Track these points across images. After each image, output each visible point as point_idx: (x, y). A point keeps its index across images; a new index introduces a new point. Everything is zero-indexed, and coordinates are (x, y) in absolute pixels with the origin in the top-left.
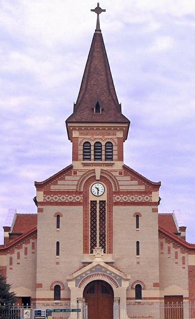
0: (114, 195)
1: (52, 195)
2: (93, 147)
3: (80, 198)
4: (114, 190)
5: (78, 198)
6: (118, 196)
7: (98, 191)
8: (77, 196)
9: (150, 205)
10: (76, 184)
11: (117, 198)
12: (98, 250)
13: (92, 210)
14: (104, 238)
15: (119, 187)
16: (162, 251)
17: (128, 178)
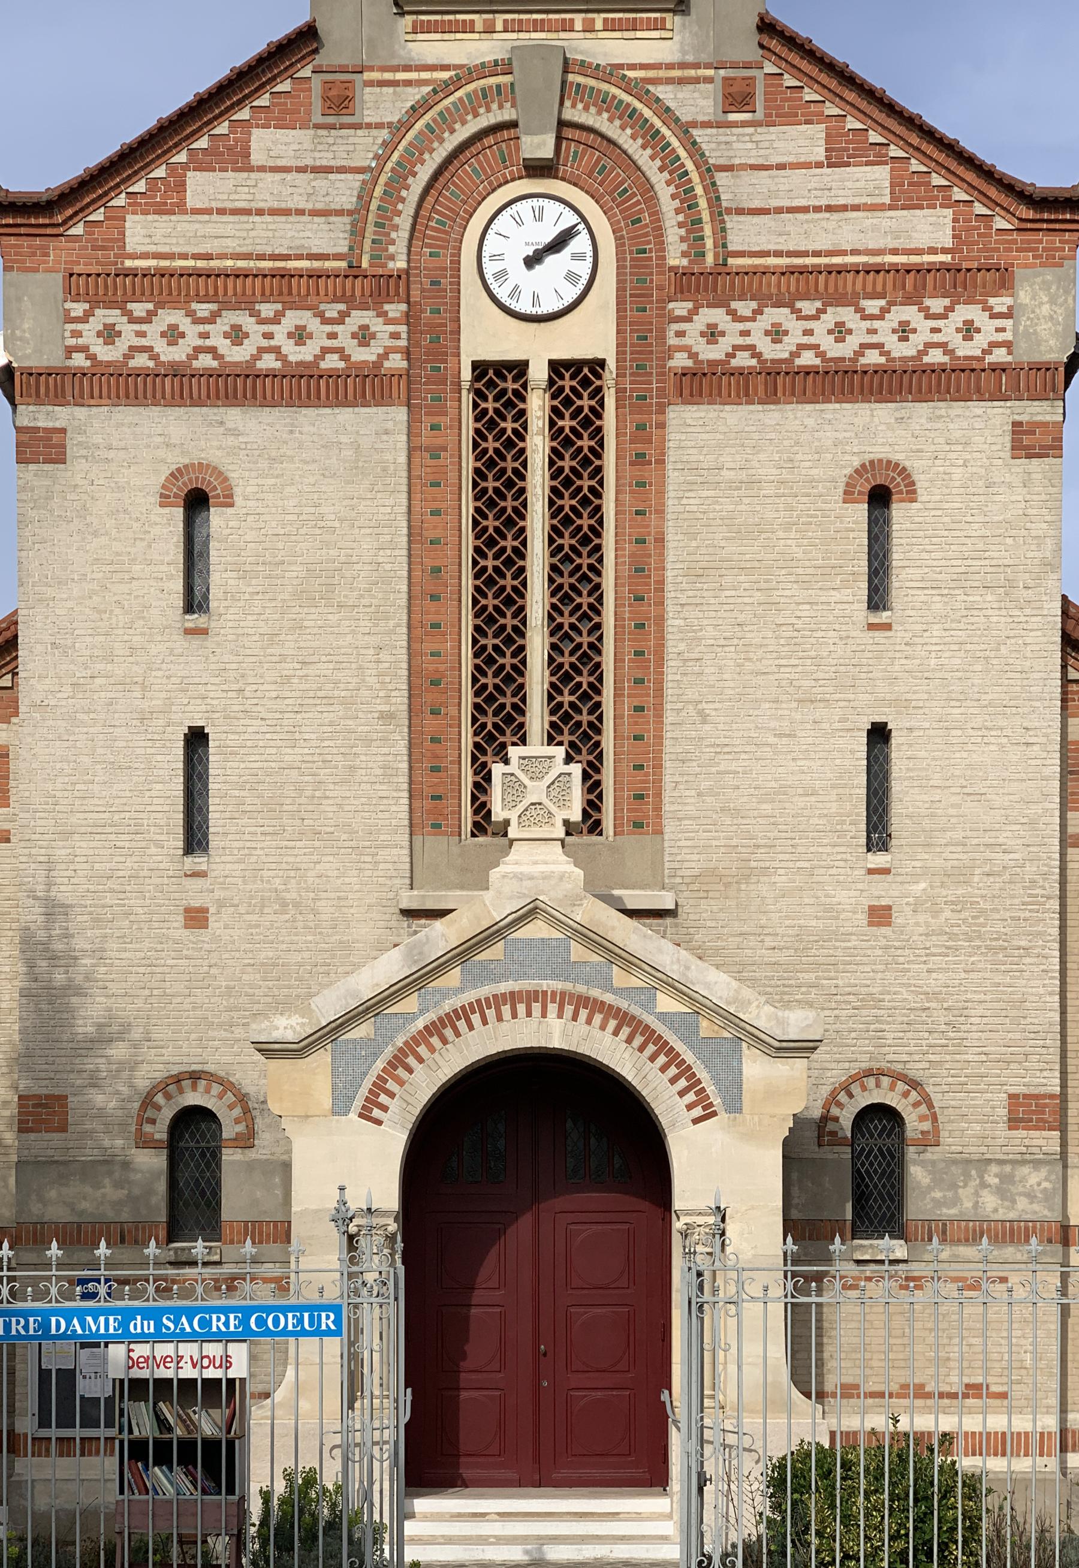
0: (680, 308)
1: (139, 309)
3: (378, 337)
4: (675, 258)
5: (364, 337)
6: (716, 315)
8: (359, 318)
9: (998, 396)
11: (700, 334)
13: (491, 445)
15: (721, 231)
17: (807, 140)
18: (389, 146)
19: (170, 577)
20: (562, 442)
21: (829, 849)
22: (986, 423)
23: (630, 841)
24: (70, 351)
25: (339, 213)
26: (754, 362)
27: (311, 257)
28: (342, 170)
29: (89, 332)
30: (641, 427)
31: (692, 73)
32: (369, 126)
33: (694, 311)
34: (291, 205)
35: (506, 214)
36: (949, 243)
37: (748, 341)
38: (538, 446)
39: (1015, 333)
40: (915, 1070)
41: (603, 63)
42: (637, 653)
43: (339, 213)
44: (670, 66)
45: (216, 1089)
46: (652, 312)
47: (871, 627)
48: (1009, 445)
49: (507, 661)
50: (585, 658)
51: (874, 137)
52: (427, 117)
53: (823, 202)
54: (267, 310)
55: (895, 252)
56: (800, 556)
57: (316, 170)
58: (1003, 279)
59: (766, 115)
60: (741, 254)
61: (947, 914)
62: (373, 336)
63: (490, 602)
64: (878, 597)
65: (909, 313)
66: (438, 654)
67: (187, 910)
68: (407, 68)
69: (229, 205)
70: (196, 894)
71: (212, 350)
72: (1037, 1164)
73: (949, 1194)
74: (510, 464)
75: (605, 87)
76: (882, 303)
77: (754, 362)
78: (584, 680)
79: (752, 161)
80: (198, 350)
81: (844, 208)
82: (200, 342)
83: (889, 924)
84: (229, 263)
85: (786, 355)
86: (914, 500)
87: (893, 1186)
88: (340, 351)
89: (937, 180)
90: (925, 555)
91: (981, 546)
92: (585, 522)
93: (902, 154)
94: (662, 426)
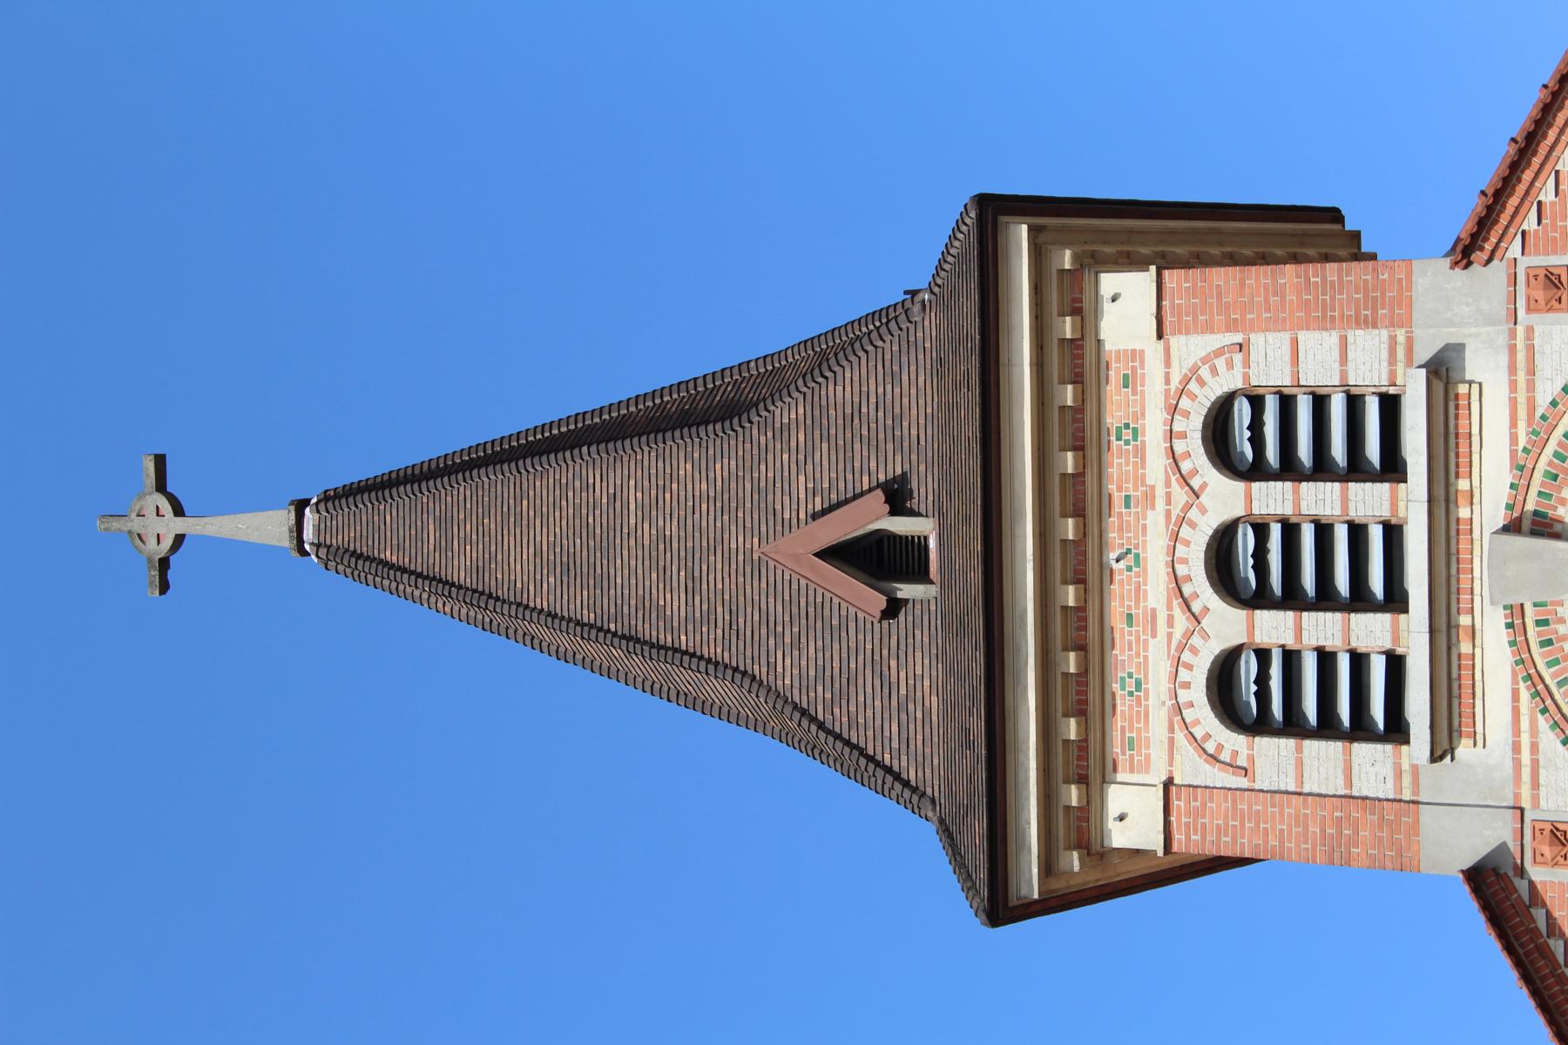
2: (1264, 617)
31: (1521, 356)
41: (1509, 480)
44: (1513, 386)
68: (1516, 748)
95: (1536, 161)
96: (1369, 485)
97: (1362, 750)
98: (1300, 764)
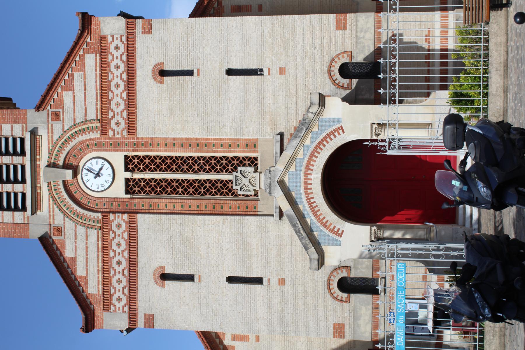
0: (111, 133)
1: (112, 291)
3: (118, 222)
5: (119, 226)
6: (113, 122)
7: (104, 177)
8: (114, 228)
10: (84, 229)
12: (246, 180)
14: (218, 160)
16: (255, 7)
17: (67, 96)
18: (69, 217)
19: (185, 285)
20: (147, 168)
21: (263, 87)
22: (143, 42)
23: (260, 148)
24: (124, 311)
25: (87, 232)
26: (125, 111)
27: (98, 241)
28: (76, 231)
29: (119, 305)
30: (143, 144)
31: (50, 130)
32: (64, 223)
33: (112, 129)
34: (85, 246)
35: (87, 184)
36: (94, 55)
37: (120, 113)
38: (148, 176)
39: (117, 34)
40: (329, 60)
41: (48, 156)
42: (206, 146)
43: (87, 232)
44: (49, 136)
45: (332, 278)
46: (112, 141)
47: (198, 75)
48: (148, 35)
49: (208, 185)
50: (207, 162)
51: (66, 77)
52: (62, 206)
53: (83, 92)
54: (112, 254)
55: (96, 70)
56: (178, 97)
57: (76, 239)
58: (103, 39)
59: (61, 108)
60: (97, 115)
61: (282, 50)
62: (119, 223)
63: (191, 190)
64: (190, 73)
65: (112, 65)
66: (206, 206)
67: (279, 284)
68: (50, 212)
69: (85, 264)
70: (274, 282)
71: (123, 270)
72: (357, 21)
73: (366, 48)
74: (153, 184)
75: (54, 155)
76: (110, 74)
77: (125, 111)
78: (213, 162)
79: (73, 112)
80: (123, 274)
81: (85, 85)
82: (121, 274)
83: (285, 68)
84: (100, 264)
85: (123, 102)
86: (163, 63)
87: (364, 65)
88: (123, 233)
89: (77, 59)
90: (178, 59)
91: (176, 42)
92: (169, 161)
93: (71, 69)
94: (142, 138)
95: (53, 89)
96: (17, 157)
97: (16, 213)
98: (3, 217)
